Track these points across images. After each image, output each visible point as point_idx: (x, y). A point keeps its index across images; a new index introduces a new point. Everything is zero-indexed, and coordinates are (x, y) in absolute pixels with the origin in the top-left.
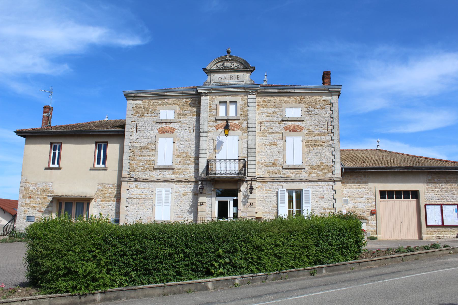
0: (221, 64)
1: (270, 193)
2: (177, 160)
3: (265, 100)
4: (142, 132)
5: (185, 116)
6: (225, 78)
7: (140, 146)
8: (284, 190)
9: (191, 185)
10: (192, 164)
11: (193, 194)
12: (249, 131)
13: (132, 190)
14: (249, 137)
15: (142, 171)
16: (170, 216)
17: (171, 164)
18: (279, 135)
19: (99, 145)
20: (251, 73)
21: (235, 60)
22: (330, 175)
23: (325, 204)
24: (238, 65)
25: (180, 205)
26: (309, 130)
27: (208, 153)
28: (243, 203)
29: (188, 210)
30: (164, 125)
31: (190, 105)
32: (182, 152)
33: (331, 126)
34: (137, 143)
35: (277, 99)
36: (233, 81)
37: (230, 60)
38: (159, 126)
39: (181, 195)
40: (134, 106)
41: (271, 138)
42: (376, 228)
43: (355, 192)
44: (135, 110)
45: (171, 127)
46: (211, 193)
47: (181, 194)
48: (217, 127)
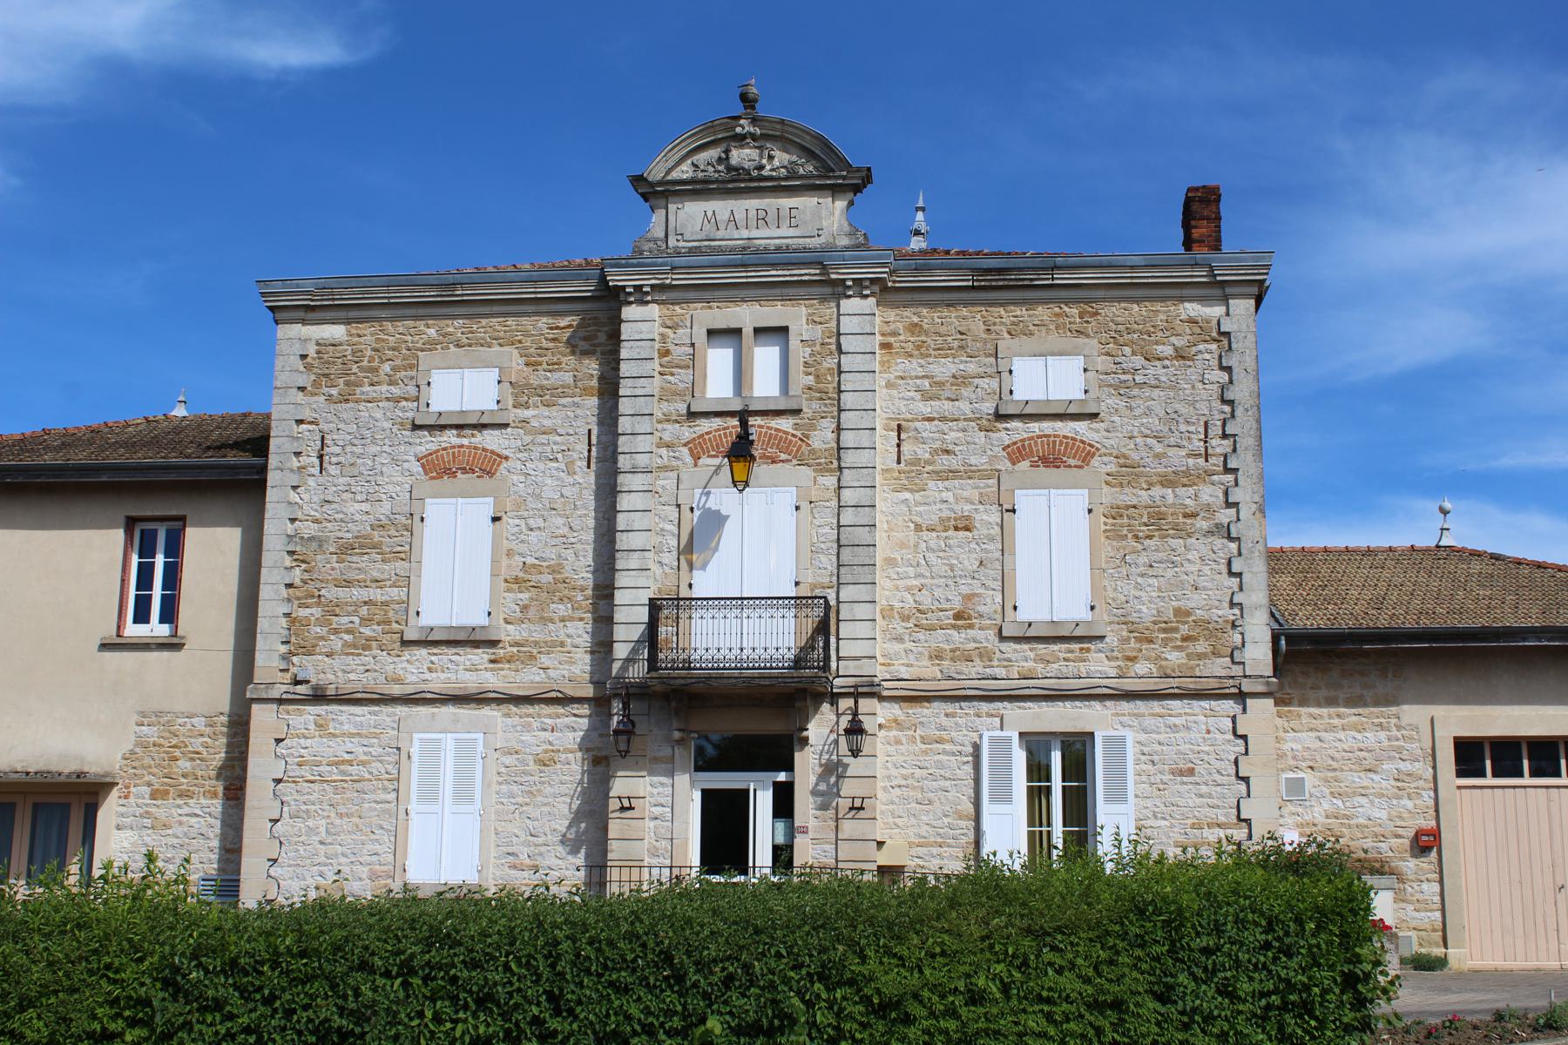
0: (713, 153)
1: (945, 752)
2: (512, 601)
3: (916, 319)
4: (347, 470)
5: (548, 396)
6: (732, 220)
7: (339, 534)
8: (1009, 739)
9: (575, 715)
10: (581, 619)
11: (583, 759)
12: (843, 465)
13: (302, 741)
14: (846, 493)
15: (347, 654)
16: (477, 862)
17: (482, 620)
18: (982, 483)
19: (142, 532)
20: (850, 195)
21: (778, 135)
22: (1219, 666)
23: (1199, 801)
24: (794, 158)
25: (525, 808)
26: (1122, 461)
27: (655, 568)
28: (819, 799)
29: (564, 836)
30: (450, 438)
31: (572, 345)
32: (534, 566)
33: (1225, 442)
34: (325, 524)
35: (972, 319)
36: (768, 236)
37: (754, 137)
38: (427, 443)
39: (532, 763)
40: (312, 350)
41: (945, 495)
42: (1438, 914)
43: (1338, 744)
44: (315, 370)
45: (484, 450)
46: (666, 751)
47: (530, 757)
48: (697, 449)
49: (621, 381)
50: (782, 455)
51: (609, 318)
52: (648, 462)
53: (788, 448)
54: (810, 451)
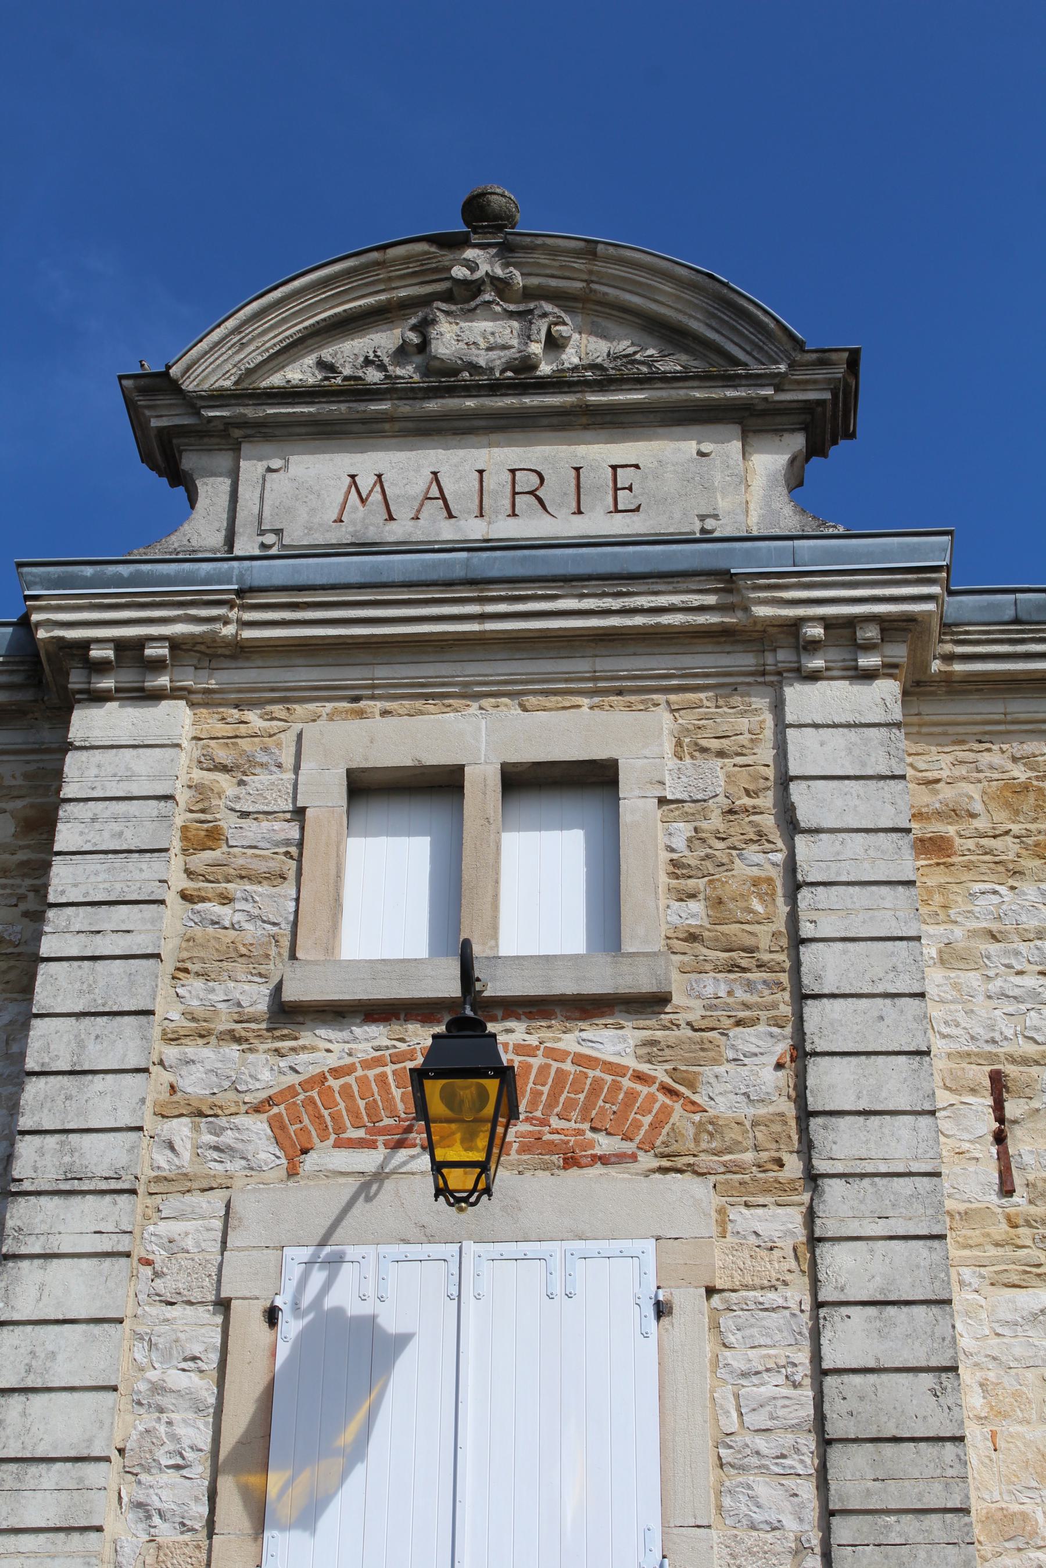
3: (1020, 773)
12: (821, 1166)
37: (501, 287)
49: (51, 914)
50: (601, 1138)
51: (26, 776)
52: (123, 1159)
53: (620, 1116)
54: (700, 1127)
